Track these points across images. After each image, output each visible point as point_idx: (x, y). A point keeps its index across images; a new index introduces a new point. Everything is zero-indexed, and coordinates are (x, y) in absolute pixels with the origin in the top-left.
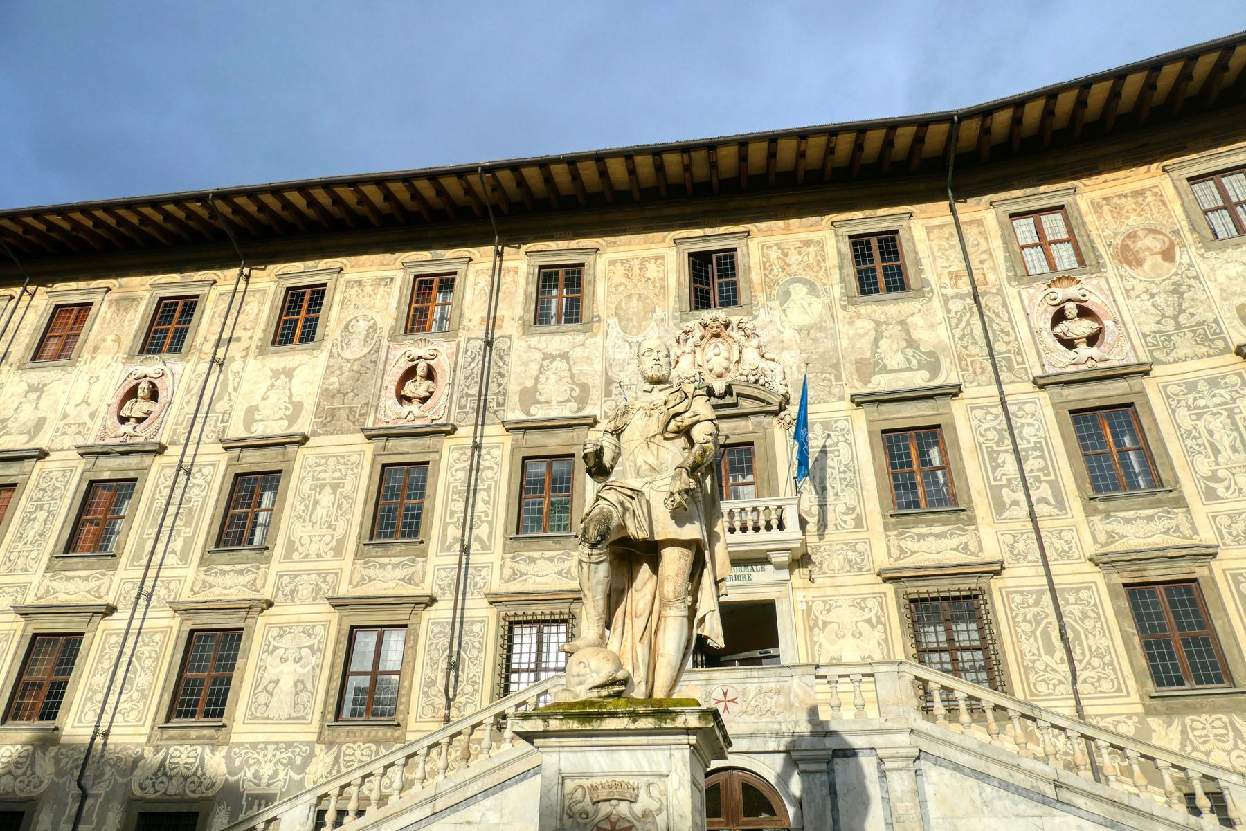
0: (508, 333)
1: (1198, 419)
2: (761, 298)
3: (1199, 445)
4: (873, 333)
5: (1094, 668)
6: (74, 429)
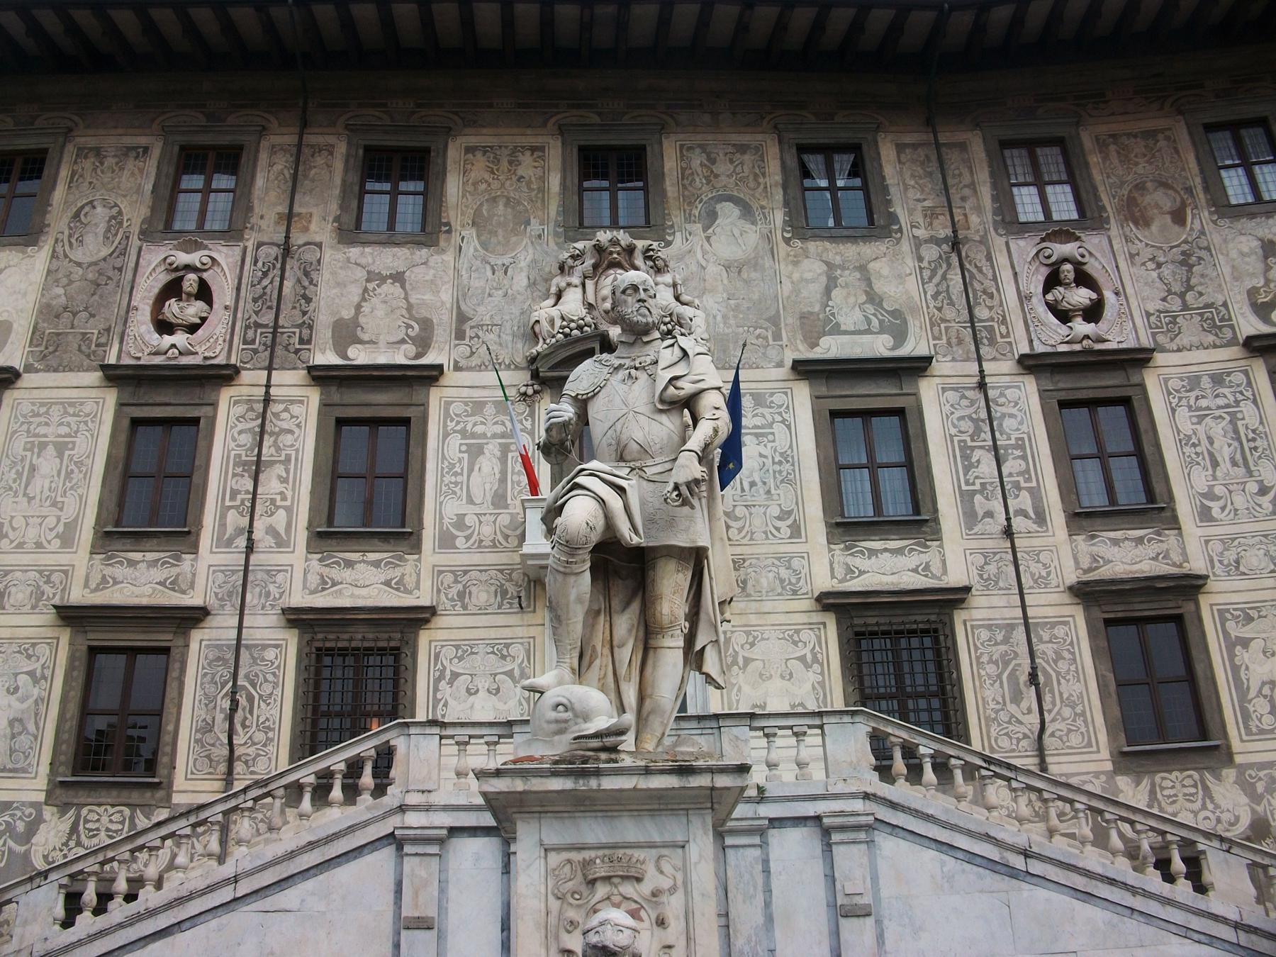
0: (318, 239)
1: (1199, 423)
2: (677, 218)
3: (1196, 453)
4: (824, 279)
5: (1064, 719)
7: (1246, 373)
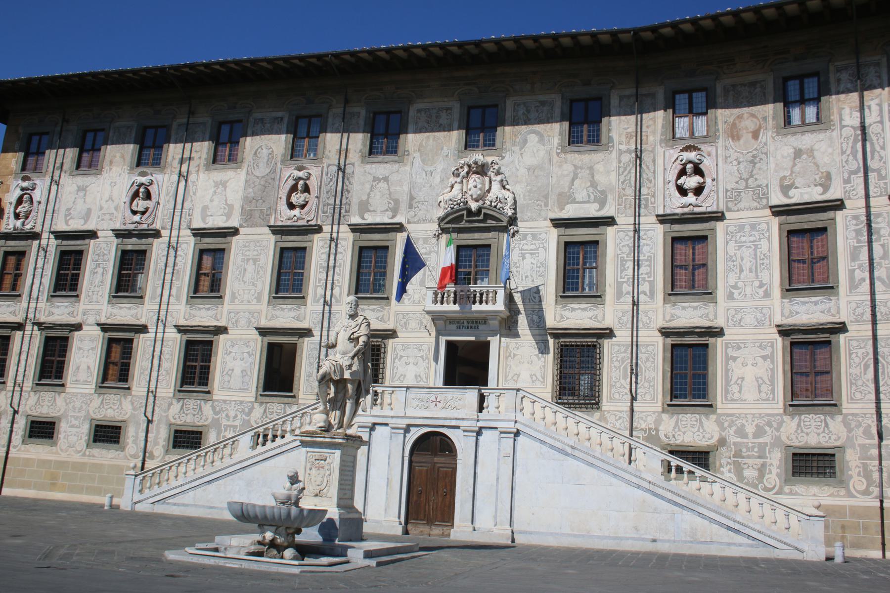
2: (508, 144)
4: (572, 175)
6: (107, 217)
7: (768, 224)
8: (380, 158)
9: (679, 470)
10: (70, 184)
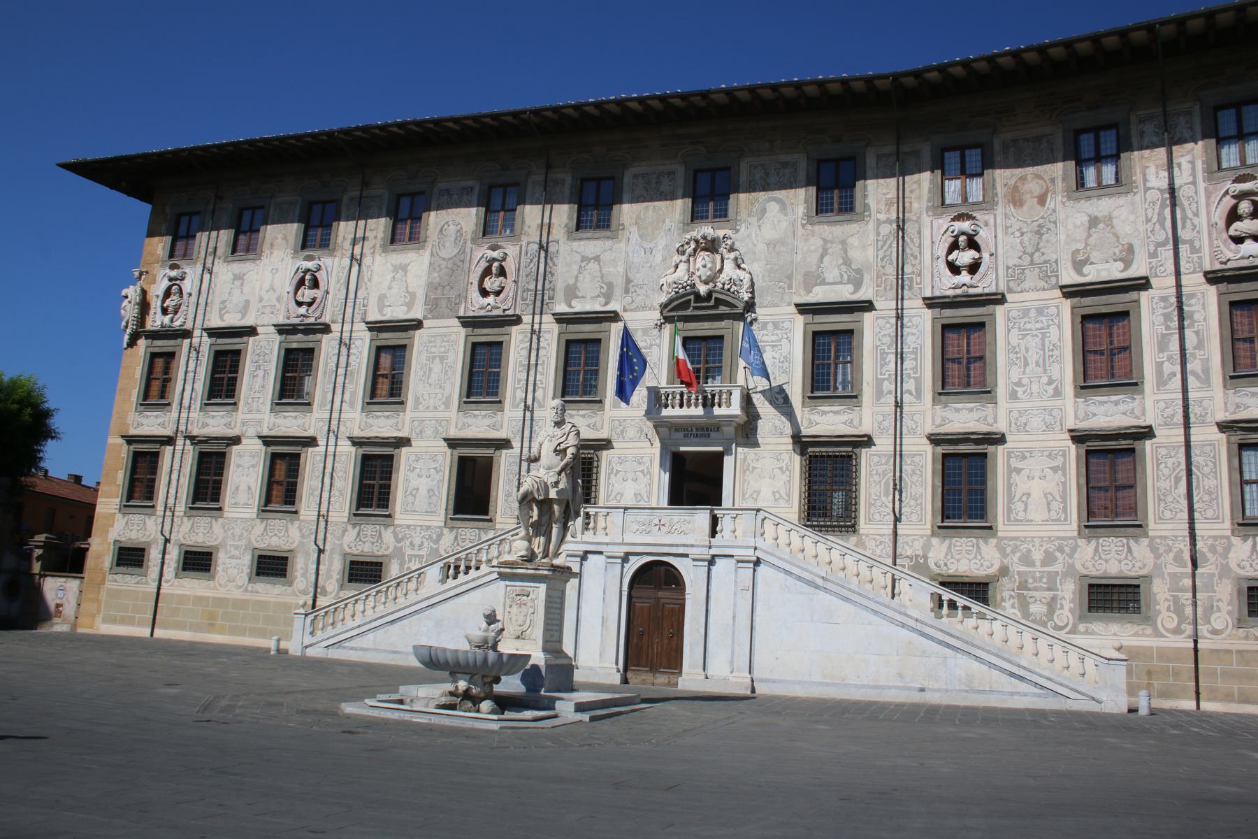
2: (743, 214)
4: (820, 250)
6: (268, 310)
7: (1058, 307)
8: (590, 234)
9: (952, 605)
10: (225, 271)
